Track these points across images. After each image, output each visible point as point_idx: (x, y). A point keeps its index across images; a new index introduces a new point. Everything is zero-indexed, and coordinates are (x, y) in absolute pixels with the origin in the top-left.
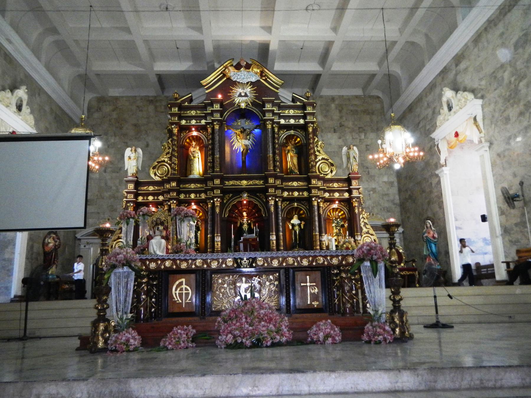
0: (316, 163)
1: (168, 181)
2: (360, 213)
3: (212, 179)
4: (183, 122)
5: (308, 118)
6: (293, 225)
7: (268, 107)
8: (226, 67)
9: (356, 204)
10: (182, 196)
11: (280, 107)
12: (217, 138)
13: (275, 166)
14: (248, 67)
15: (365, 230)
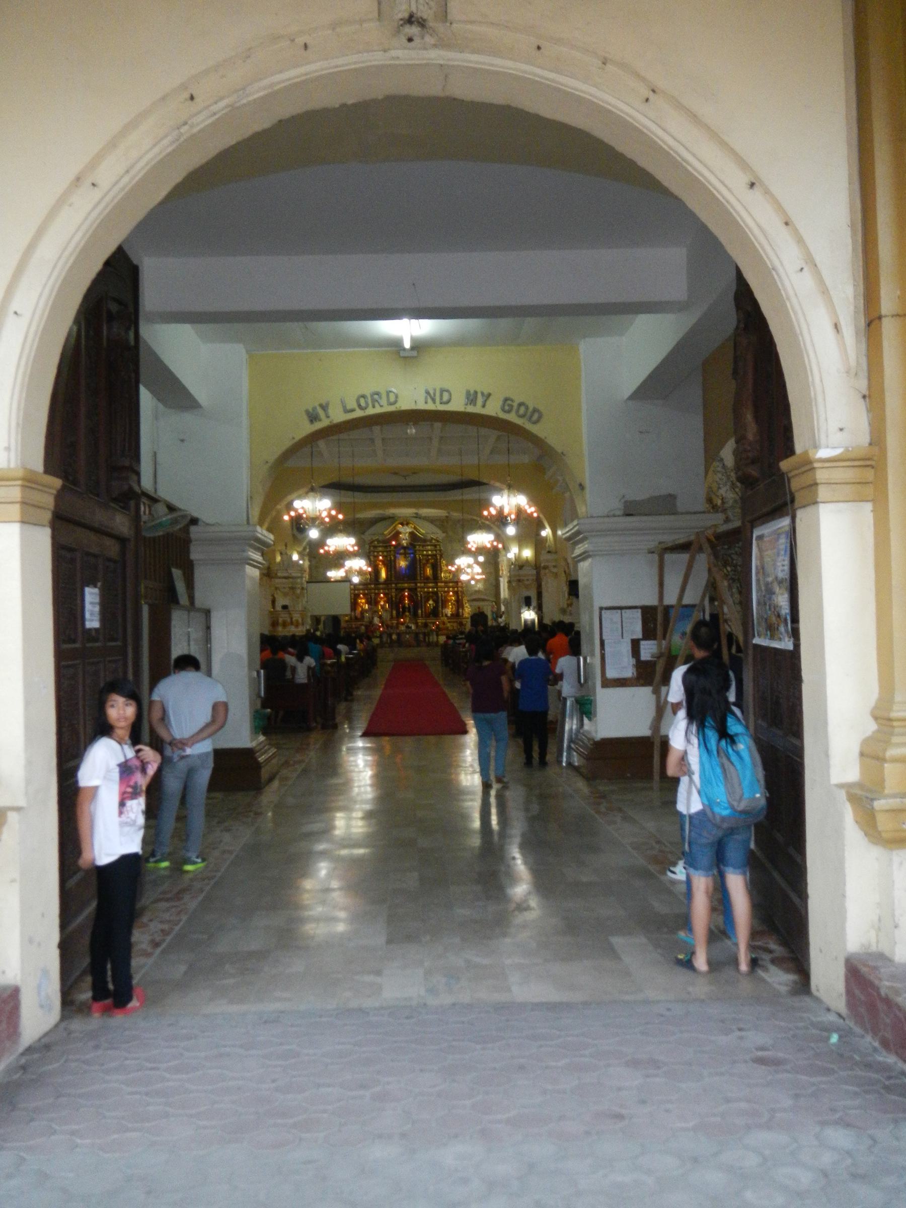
0: (441, 572)
1: (370, 584)
2: (462, 598)
3: (391, 584)
4: (376, 554)
5: (438, 552)
6: (430, 605)
7: (417, 547)
8: (396, 526)
9: (460, 594)
10: (376, 591)
11: (423, 546)
12: (393, 563)
13: (421, 577)
14: (407, 524)
15: (465, 606)
